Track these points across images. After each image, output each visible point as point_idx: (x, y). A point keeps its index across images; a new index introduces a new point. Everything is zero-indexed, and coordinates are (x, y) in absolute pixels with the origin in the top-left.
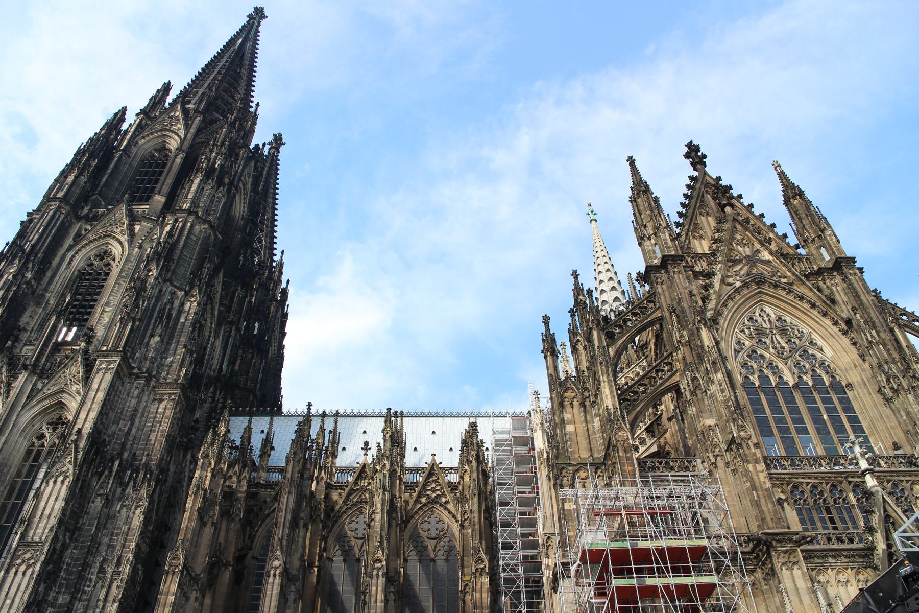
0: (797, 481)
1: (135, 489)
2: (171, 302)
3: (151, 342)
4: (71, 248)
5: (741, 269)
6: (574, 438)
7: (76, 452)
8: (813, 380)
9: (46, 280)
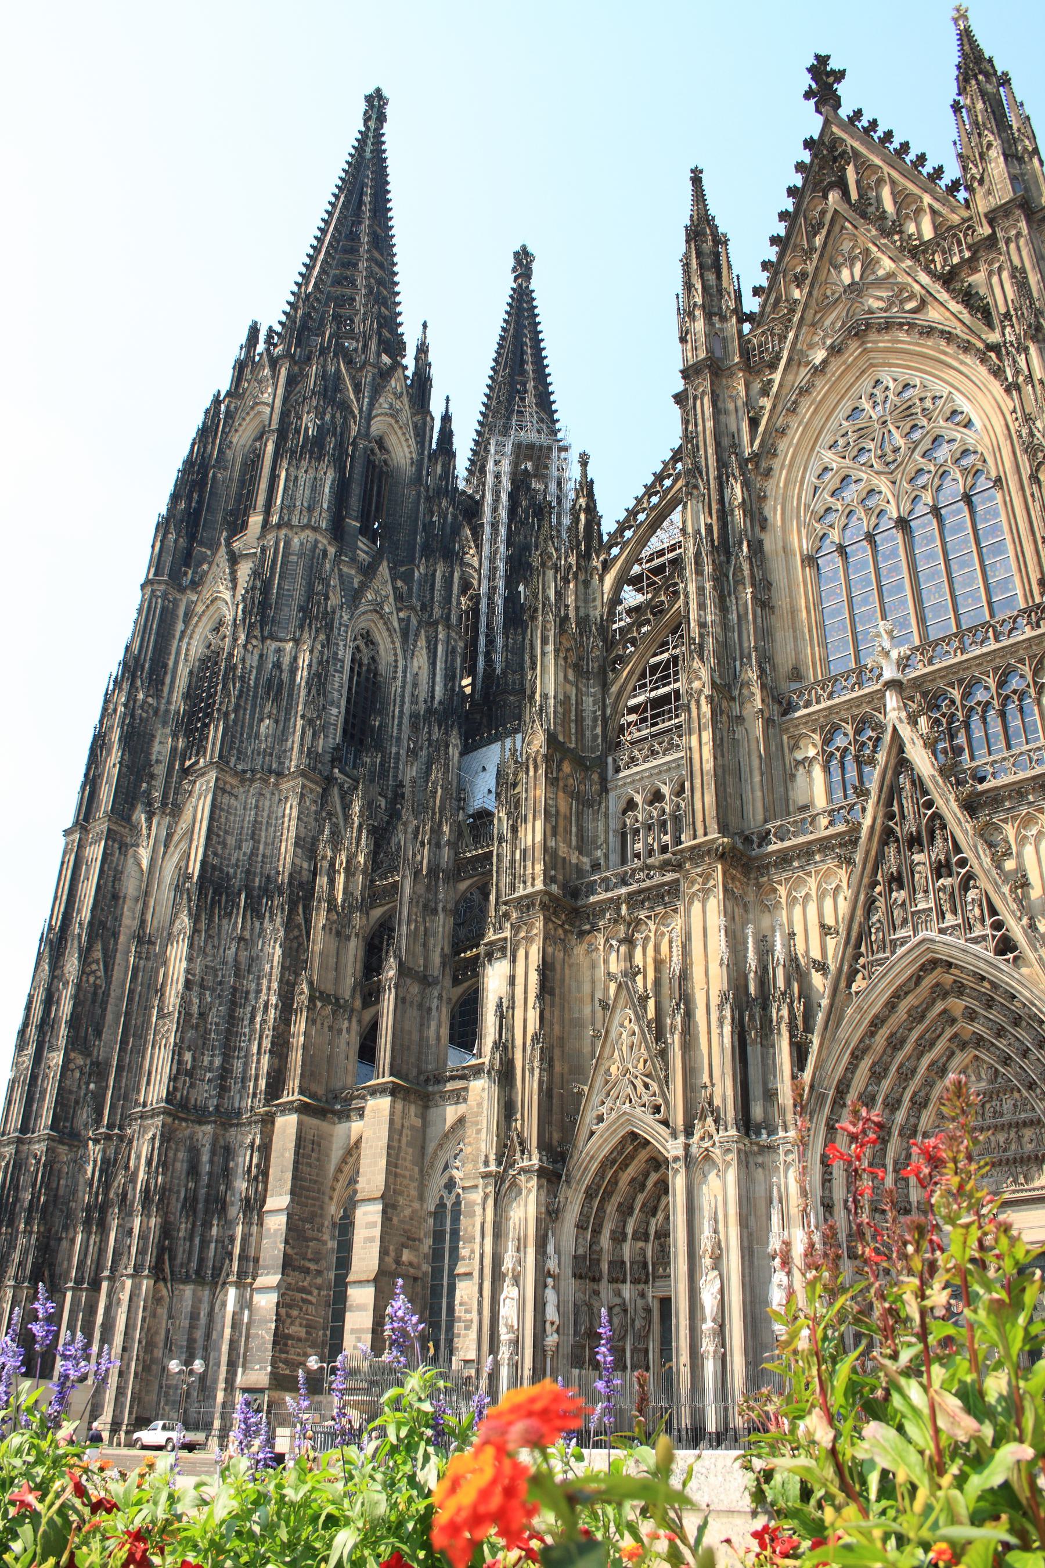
1: (272, 920)
2: (278, 665)
3: (263, 729)
9: (166, 689)
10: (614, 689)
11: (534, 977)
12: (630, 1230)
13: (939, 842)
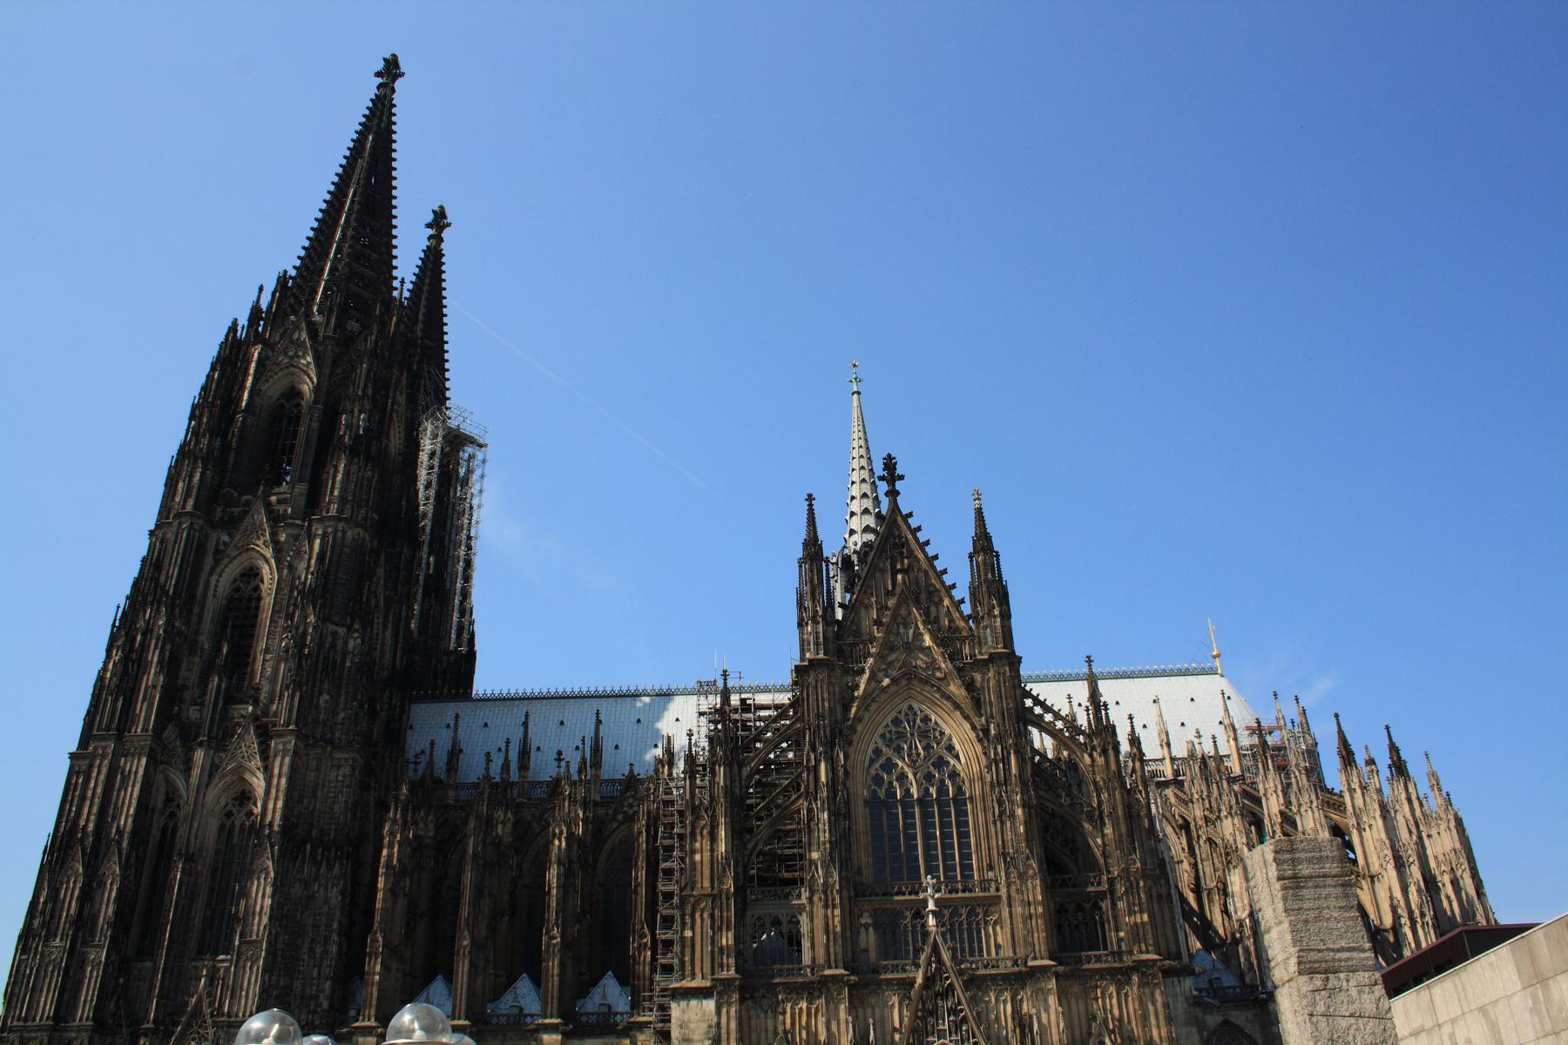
1: (330, 868)
2: (333, 646)
4: (213, 570)
7: (272, 846)
8: (939, 792)
9: (194, 619)
10: (750, 846)
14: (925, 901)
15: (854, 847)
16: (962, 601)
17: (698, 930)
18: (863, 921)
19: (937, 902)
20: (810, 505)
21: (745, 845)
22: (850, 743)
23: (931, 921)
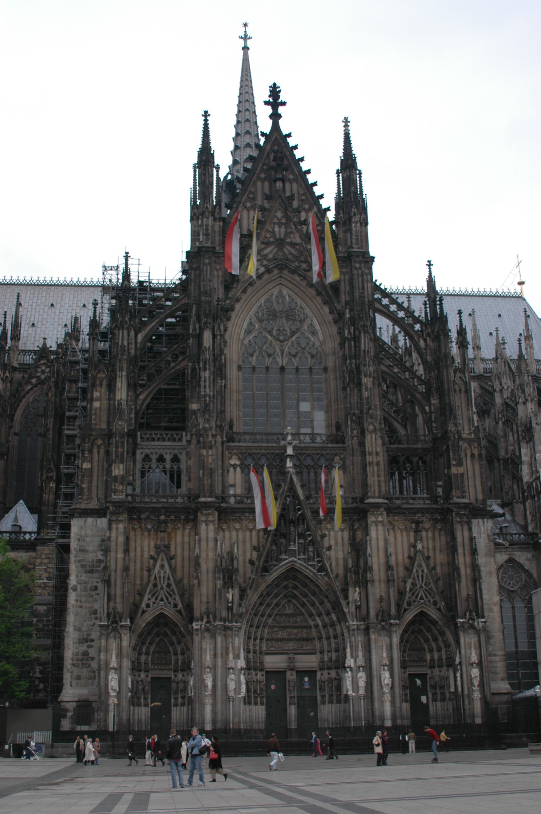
0: (251, 451)
5: (270, 252)
6: (98, 412)
10: (142, 397)
11: (121, 539)
12: (144, 650)
13: (301, 527)
14: (285, 448)
15: (227, 402)
16: (328, 209)
17: (95, 464)
18: (232, 462)
19: (295, 448)
20: (206, 120)
21: (137, 396)
22: (229, 319)
23: (289, 464)
